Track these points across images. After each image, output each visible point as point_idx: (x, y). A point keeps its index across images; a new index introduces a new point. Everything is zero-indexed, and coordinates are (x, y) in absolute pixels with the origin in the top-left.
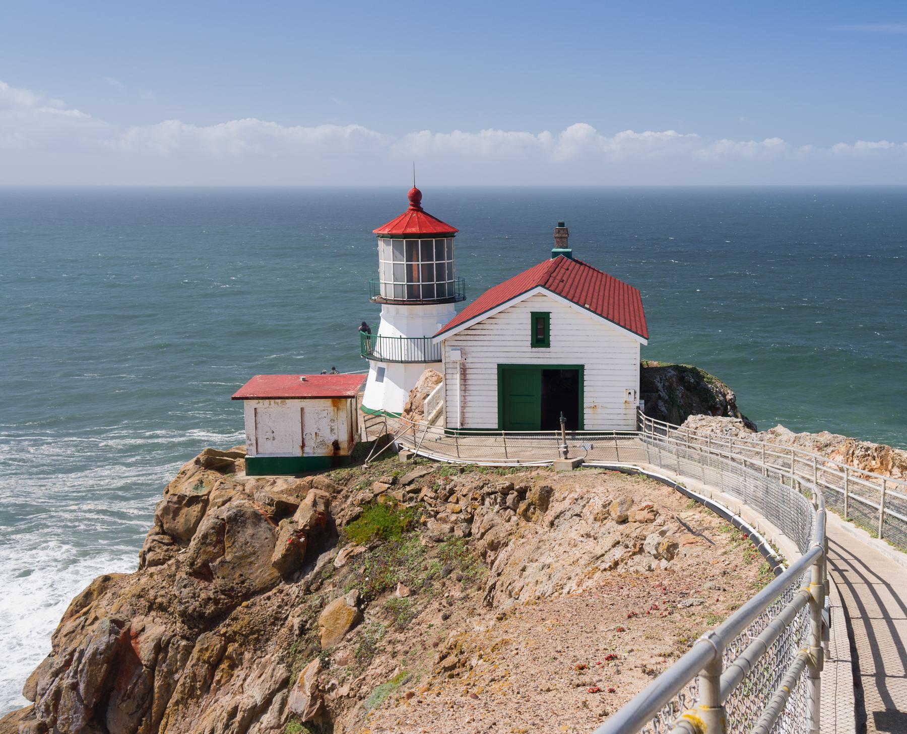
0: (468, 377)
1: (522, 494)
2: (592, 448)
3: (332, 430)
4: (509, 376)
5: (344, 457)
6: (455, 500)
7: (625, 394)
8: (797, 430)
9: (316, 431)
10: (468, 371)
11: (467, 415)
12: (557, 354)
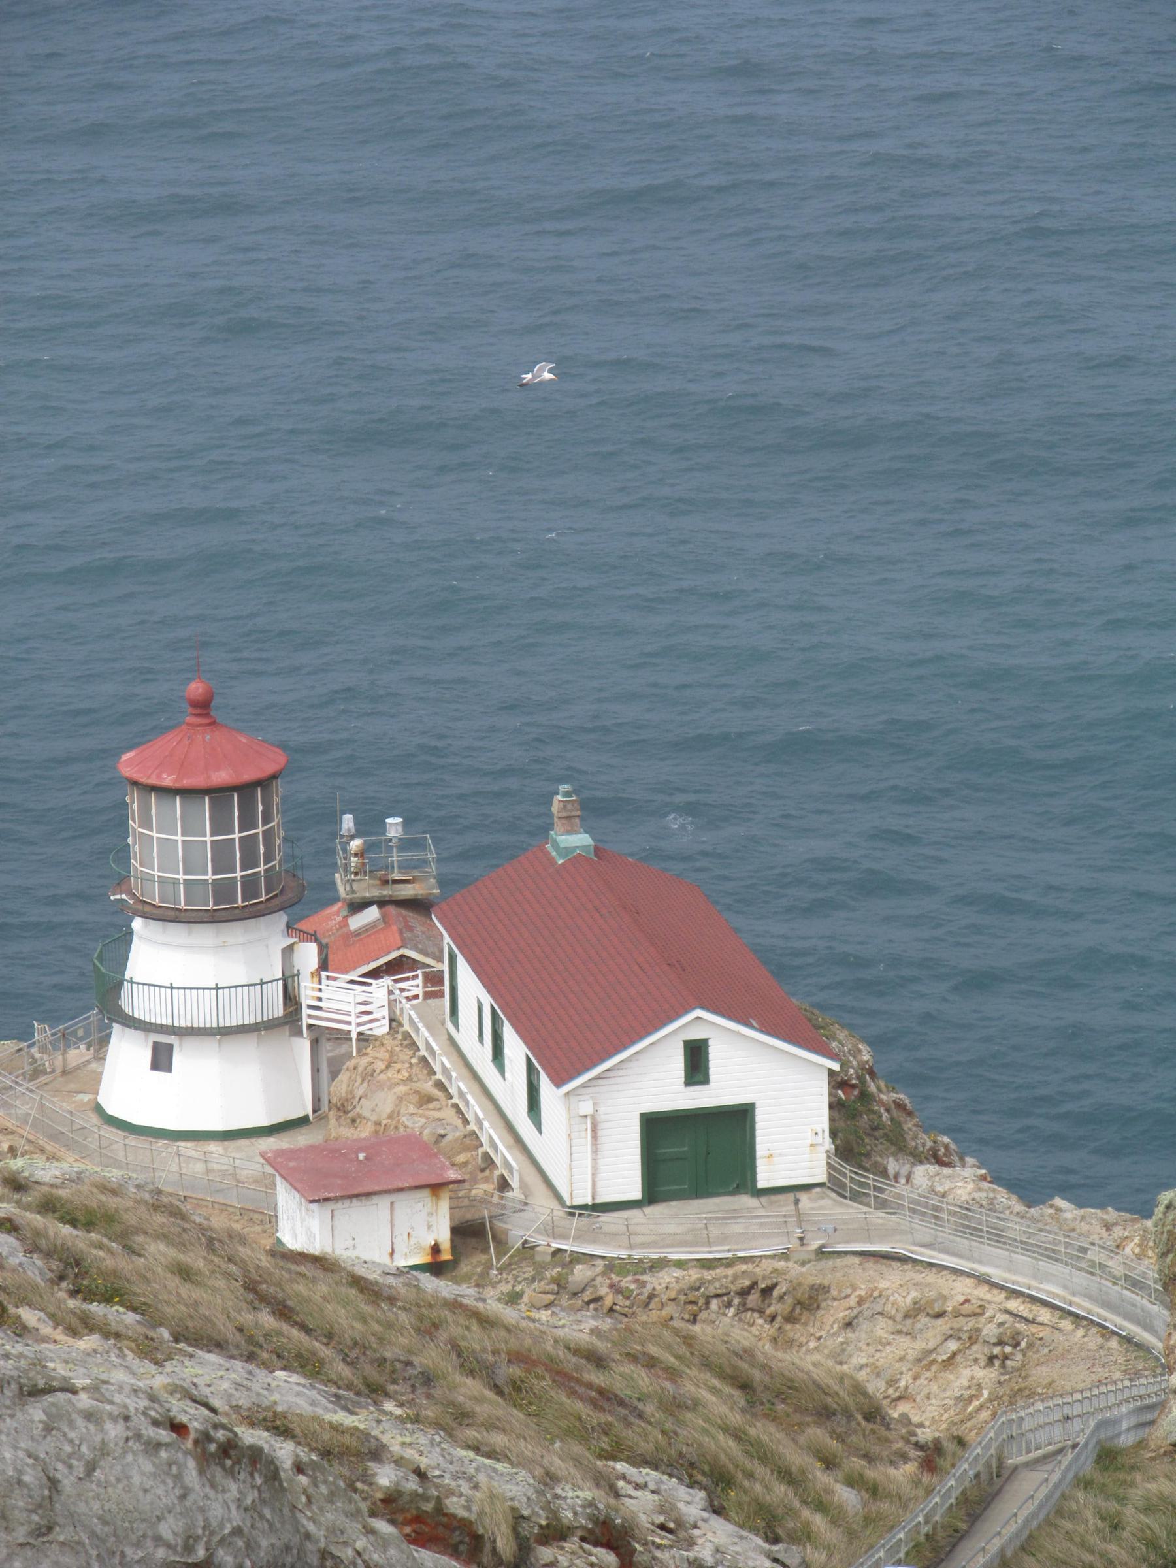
0: (600, 1133)
1: (767, 1292)
2: (835, 1230)
3: (429, 1227)
4: (655, 1126)
5: (446, 1262)
6: (659, 1306)
7: (810, 1134)
9: (409, 1230)
10: (601, 1126)
11: (599, 1184)
12: (719, 1092)
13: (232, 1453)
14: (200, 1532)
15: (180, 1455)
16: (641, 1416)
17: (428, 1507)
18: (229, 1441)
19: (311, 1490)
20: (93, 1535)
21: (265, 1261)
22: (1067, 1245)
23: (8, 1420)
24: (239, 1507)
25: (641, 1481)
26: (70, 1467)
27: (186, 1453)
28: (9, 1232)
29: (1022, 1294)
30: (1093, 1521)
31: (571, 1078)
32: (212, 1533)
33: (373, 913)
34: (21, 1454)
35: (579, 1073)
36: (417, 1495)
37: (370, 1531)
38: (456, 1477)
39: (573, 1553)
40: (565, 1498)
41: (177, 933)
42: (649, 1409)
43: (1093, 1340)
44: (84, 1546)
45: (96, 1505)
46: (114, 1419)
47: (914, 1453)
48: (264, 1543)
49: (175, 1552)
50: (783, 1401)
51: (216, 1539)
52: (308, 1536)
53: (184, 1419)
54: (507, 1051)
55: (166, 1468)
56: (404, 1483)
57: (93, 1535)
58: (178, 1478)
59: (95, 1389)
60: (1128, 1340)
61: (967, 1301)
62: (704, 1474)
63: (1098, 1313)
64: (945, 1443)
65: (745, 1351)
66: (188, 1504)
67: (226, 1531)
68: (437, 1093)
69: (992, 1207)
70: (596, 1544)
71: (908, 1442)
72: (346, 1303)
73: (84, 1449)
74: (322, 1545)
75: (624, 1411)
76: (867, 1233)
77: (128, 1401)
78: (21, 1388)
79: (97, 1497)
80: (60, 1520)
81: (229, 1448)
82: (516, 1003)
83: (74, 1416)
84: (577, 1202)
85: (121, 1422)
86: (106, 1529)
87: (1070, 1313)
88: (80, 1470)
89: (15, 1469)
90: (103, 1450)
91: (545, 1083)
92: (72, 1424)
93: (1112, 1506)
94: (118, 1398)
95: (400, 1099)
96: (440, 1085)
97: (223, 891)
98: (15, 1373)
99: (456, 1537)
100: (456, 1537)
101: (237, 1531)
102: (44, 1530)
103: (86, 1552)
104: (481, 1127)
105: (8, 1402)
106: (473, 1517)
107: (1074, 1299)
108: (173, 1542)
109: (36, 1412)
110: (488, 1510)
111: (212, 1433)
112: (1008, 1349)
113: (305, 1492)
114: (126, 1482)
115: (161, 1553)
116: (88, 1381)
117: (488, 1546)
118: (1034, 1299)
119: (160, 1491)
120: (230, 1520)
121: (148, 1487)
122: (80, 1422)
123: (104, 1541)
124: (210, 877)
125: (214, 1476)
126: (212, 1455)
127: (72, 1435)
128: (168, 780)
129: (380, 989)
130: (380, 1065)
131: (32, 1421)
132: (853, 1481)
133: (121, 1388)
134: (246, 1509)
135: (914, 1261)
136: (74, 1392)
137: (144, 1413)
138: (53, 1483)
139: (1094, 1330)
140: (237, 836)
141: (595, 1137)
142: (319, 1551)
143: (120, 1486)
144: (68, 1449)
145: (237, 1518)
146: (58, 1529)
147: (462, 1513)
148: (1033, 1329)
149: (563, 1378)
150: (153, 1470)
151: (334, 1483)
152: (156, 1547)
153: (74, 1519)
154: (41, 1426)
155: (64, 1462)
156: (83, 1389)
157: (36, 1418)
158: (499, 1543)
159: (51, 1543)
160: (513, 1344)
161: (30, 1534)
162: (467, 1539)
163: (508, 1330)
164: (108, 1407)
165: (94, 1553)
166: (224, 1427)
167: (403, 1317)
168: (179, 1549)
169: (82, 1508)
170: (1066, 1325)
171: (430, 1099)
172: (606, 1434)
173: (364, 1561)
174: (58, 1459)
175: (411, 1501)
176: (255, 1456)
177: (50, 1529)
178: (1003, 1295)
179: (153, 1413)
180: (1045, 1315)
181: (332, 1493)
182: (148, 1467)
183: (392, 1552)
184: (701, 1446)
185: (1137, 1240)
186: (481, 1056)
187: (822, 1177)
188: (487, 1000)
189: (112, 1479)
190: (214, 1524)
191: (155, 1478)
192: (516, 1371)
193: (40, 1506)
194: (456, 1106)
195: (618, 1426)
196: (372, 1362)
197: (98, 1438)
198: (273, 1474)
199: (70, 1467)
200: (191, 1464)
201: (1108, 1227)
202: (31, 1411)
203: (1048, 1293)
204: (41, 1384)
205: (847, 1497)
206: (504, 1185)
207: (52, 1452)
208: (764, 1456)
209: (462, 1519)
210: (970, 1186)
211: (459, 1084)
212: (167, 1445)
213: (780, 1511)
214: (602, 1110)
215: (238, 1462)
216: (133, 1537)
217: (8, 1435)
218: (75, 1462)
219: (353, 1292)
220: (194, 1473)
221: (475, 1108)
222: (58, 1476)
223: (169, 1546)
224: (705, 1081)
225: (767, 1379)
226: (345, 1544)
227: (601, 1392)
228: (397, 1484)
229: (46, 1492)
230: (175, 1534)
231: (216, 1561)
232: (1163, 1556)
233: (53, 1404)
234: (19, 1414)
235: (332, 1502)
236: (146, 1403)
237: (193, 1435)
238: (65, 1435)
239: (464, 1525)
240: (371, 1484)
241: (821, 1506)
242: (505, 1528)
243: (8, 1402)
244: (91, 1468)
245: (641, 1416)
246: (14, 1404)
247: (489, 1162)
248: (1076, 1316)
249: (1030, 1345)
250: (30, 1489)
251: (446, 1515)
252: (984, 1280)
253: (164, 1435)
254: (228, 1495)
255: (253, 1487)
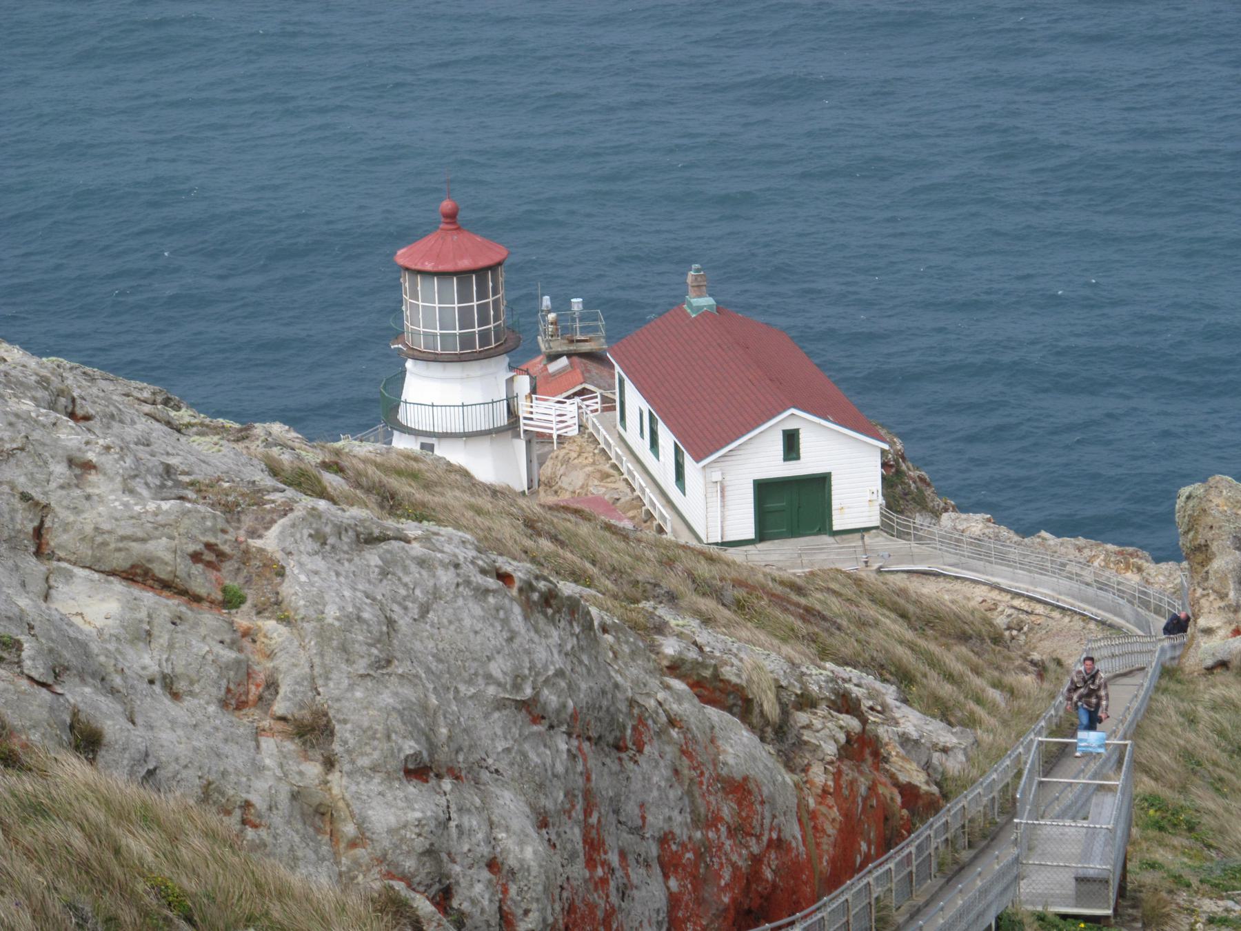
4: (765, 489)
7: (868, 493)
8: (1058, 536)
10: (727, 489)
12: (805, 466)
13: (553, 602)
14: (527, 672)
15: (507, 601)
16: (839, 628)
17: (707, 673)
18: (550, 591)
19: (616, 647)
20: (428, 670)
21: (538, 509)
22: (1052, 562)
23: (346, 564)
24: (560, 652)
25: (846, 676)
26: (406, 608)
27: (512, 599)
28: (336, 473)
29: (1023, 595)
30: (1175, 718)
31: (707, 456)
32: (538, 674)
33: (564, 361)
34: (359, 594)
35: (711, 453)
36: (698, 663)
37: (667, 687)
38: (723, 652)
39: (824, 717)
40: (810, 675)
41: (436, 369)
42: (844, 623)
43: (1077, 624)
44: (421, 679)
45: (431, 644)
46: (445, 566)
47: (1031, 668)
48: (583, 686)
49: (505, 690)
50: (932, 628)
51: (541, 679)
52: (616, 686)
53: (508, 569)
54: (661, 441)
55: (494, 612)
56: (686, 653)
57: (428, 670)
58: (505, 622)
59: (426, 539)
60: (1103, 623)
61: (984, 601)
62: (891, 674)
63: (1079, 606)
64: (1047, 663)
65: (901, 590)
66: (515, 646)
67: (550, 673)
68: (612, 471)
69: (997, 537)
70: (839, 712)
71: (1025, 660)
72: (604, 541)
73: (418, 592)
74: (630, 694)
75: (827, 625)
76: (912, 558)
77: (457, 551)
78: (358, 536)
79: (431, 636)
80: (399, 655)
81: (550, 598)
82: (668, 406)
83: (408, 562)
84: (711, 541)
85: (452, 569)
86: (440, 666)
87: (1058, 607)
88: (415, 611)
89: (354, 606)
90: (436, 594)
91: (688, 460)
92: (405, 569)
93: (1184, 706)
94: (447, 548)
95: (589, 476)
96: (615, 467)
97: (466, 341)
98: (352, 522)
99: (731, 700)
100: (731, 700)
101: (560, 673)
102: (383, 663)
103: (424, 686)
104: (644, 493)
105: (346, 548)
106: (744, 684)
107: (1062, 597)
108: (502, 680)
109: (373, 557)
110: (755, 678)
111: (534, 583)
112: (1015, 633)
113: (611, 648)
114: (457, 624)
115: (491, 690)
116: (420, 532)
117: (757, 710)
118: (1031, 599)
119: (489, 633)
120: (553, 663)
121: (478, 629)
122: (413, 568)
123: (439, 678)
124: (457, 331)
125: (537, 622)
126: (534, 602)
127: (406, 579)
128: (429, 266)
129: (571, 408)
130: (574, 455)
131: (369, 566)
132: (997, 685)
133: (450, 540)
134: (567, 654)
135: (945, 575)
136: (408, 542)
137: (472, 562)
138: (391, 622)
139: (1077, 617)
140: (475, 303)
141: (723, 496)
142: (627, 699)
143: (452, 628)
144: (403, 592)
145: (559, 662)
146: (396, 662)
147: (734, 680)
148: (1033, 618)
149: (778, 600)
150: (482, 613)
151: (634, 643)
152: (487, 684)
153: (410, 655)
154: (377, 570)
155: (400, 604)
156: (415, 539)
157: (373, 563)
158: (766, 707)
159: (390, 675)
160: (734, 574)
161: (370, 666)
162: (740, 703)
163: (728, 565)
164: (439, 555)
165: (431, 686)
166: (546, 579)
167: (647, 552)
168: (508, 686)
169: (418, 645)
170: (1056, 614)
171: (608, 476)
172: (814, 642)
173: (665, 711)
174: (394, 601)
175: (692, 669)
176: (573, 608)
177: (389, 662)
178: (1009, 597)
179: (480, 563)
180: (1040, 609)
181: (633, 652)
182: (477, 611)
183: (686, 705)
184: (887, 651)
185: (1102, 557)
186: (642, 446)
187: (877, 523)
188: (646, 407)
189: (445, 621)
190: (539, 666)
191: (484, 621)
192: (741, 593)
193: (379, 641)
194: (626, 480)
195: (824, 635)
196: (629, 582)
197: (431, 583)
198: (588, 626)
199: (406, 608)
200: (517, 610)
201: (1080, 550)
202: (368, 556)
203: (1041, 594)
204: (376, 532)
205: (995, 695)
206: (661, 530)
207: (388, 594)
208: (933, 662)
209: (736, 685)
210: (981, 526)
211: (627, 465)
212: (494, 591)
213: (951, 703)
214: (727, 478)
215: (559, 611)
216: (466, 675)
217: (347, 577)
218: (410, 605)
219: (607, 534)
220: (520, 618)
221: (640, 480)
222: (395, 616)
223: (499, 684)
224: (798, 458)
225: (918, 611)
226: (648, 695)
227: (808, 610)
228: (680, 653)
229: (385, 629)
230: (505, 673)
231: (542, 699)
232: (1230, 743)
233: (388, 551)
234: (356, 559)
235: (633, 660)
236: (474, 553)
237: (517, 584)
238: (400, 579)
239: (738, 690)
240: (658, 653)
241: (979, 701)
242: (771, 695)
243: (346, 548)
244: (425, 610)
245: (839, 628)
246: (352, 549)
247: (650, 516)
248: (1063, 609)
249: (1031, 629)
250: (369, 625)
251: (722, 681)
252: (995, 587)
253: (492, 583)
254: (550, 641)
255: (572, 635)
